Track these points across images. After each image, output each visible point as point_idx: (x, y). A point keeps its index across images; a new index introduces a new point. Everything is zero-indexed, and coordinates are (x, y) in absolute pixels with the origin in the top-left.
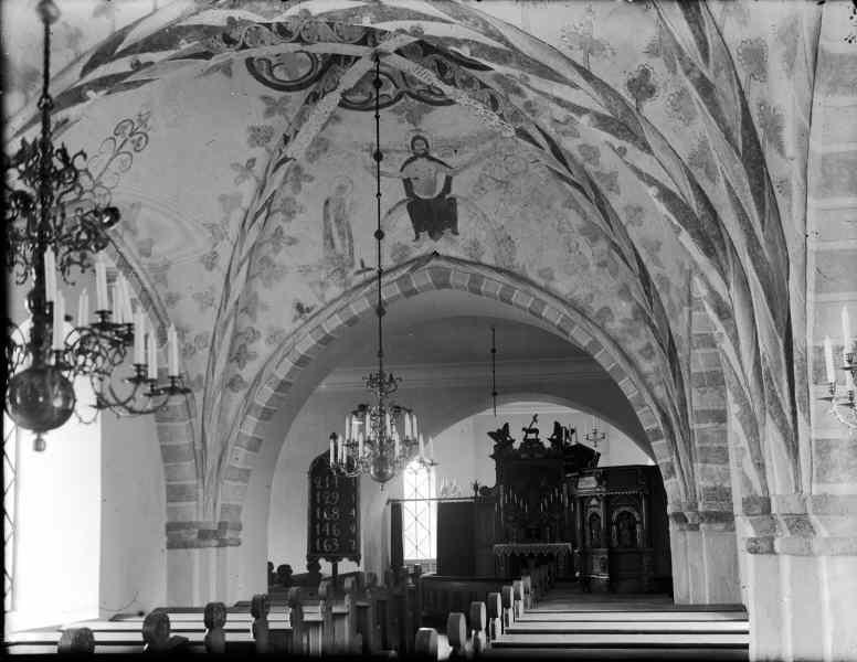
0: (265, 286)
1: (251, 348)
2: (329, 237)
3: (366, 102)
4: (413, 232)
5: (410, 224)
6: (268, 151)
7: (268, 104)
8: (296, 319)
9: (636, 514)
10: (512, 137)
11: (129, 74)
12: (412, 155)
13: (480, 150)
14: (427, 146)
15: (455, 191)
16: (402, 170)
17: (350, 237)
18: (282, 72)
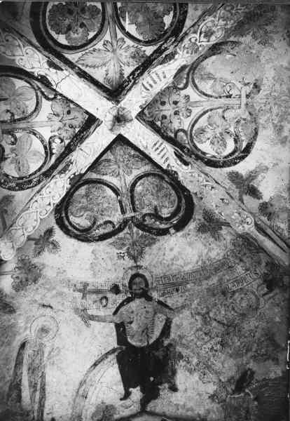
3: (88, 230)
4: (121, 388)
5: (119, 377)
14: (147, 285)
16: (115, 313)
18: (13, 166)
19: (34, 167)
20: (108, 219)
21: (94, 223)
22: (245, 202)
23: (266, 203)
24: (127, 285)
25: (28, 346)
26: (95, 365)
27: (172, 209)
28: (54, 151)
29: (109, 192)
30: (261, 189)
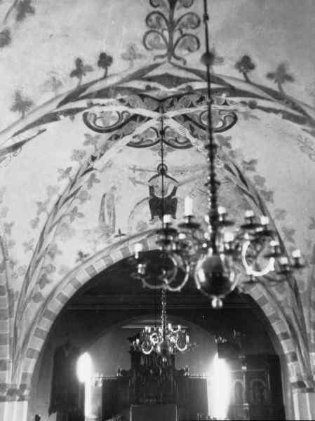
0: (62, 240)
1: (49, 277)
2: (102, 215)
3: (138, 143)
4: (150, 215)
5: (149, 211)
6: (80, 163)
7: (87, 138)
8: (77, 261)
9: (263, 382)
10: (221, 169)
11: (85, 109)
13: (196, 174)
15: (178, 195)
16: (149, 181)
26: (138, 204)
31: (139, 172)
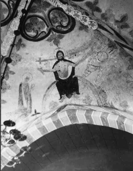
5: (58, 92)
10: (96, 30)
12: (57, 60)
14: (63, 55)
15: (77, 74)
17: (31, 100)
19: (6, 15)
20: (42, 30)
21: (37, 33)
22: (95, 15)
23: (104, 13)
24: (56, 56)
25: (22, 85)
26: (49, 88)
27: (67, 22)
28: (11, 7)
29: (40, 20)
30: (101, 7)
31: (44, 63)
